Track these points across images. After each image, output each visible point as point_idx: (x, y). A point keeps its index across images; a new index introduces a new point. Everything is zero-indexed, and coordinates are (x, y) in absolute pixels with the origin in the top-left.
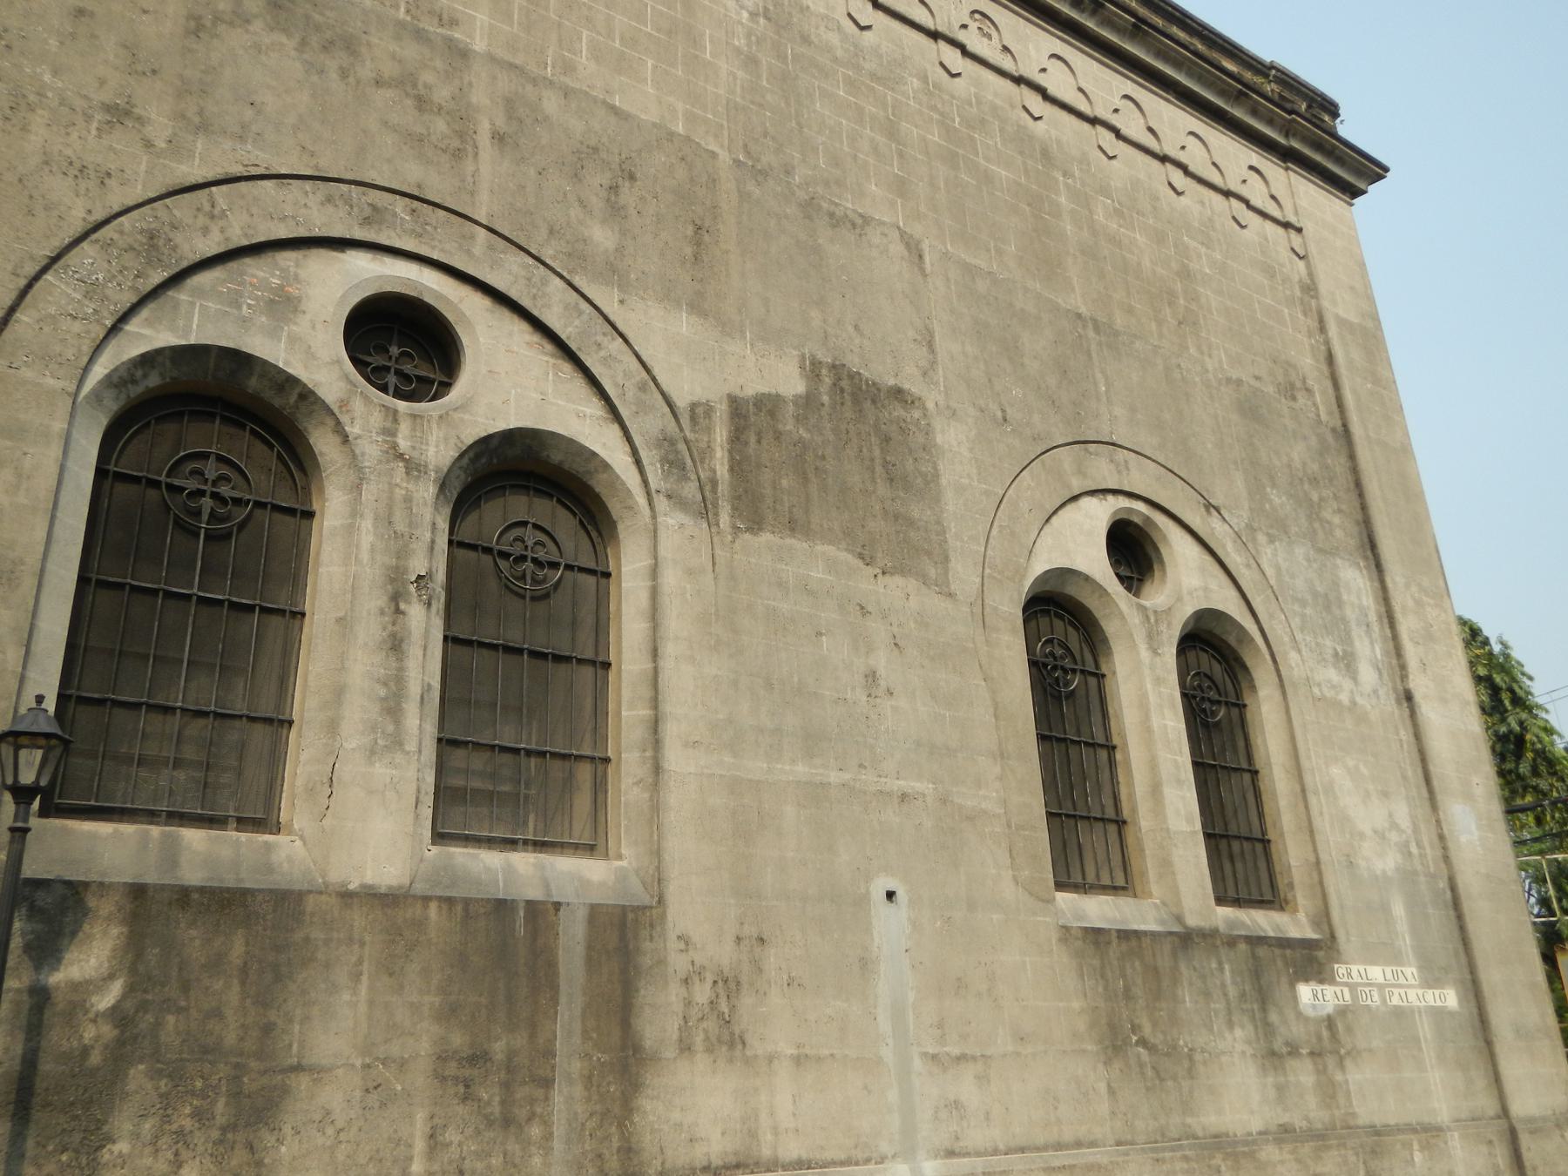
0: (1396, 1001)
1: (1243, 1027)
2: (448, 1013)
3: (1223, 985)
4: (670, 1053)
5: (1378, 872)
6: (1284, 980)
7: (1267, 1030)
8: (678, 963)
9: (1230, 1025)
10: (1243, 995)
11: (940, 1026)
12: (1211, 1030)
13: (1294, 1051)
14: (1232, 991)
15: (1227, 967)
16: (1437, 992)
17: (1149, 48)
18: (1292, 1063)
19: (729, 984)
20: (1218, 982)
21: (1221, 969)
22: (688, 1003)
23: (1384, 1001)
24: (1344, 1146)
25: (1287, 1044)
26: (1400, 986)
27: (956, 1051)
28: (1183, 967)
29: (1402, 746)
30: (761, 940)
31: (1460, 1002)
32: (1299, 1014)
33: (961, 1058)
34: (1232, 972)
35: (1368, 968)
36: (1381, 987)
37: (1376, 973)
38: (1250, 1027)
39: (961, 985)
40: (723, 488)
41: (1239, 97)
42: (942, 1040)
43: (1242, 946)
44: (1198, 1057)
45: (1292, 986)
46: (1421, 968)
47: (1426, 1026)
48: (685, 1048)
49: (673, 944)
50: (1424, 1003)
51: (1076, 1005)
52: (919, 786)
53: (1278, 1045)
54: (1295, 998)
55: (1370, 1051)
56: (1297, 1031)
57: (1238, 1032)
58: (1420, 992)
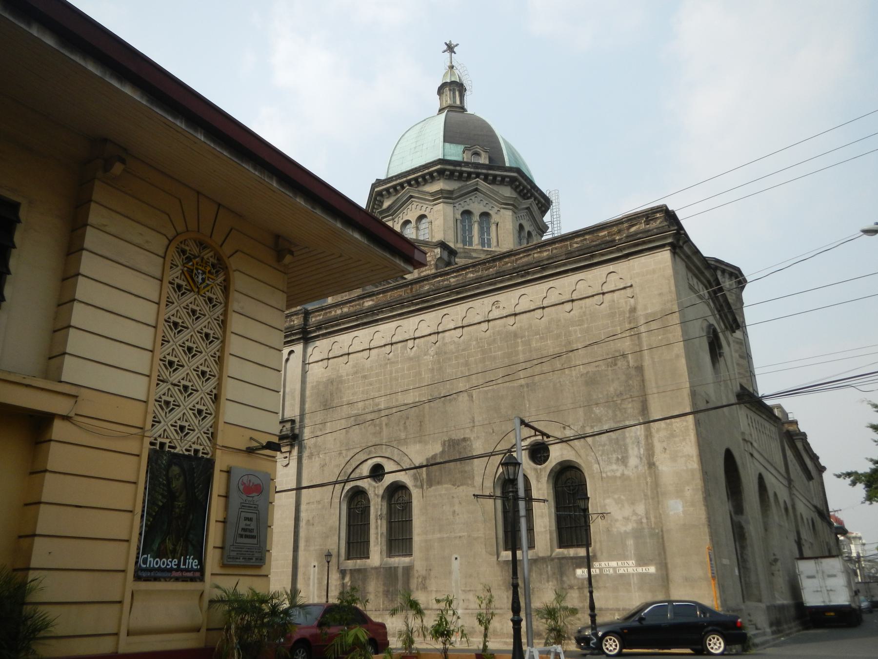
0: (620, 572)
1: (552, 582)
2: (384, 585)
3: (547, 571)
4: (415, 590)
5: (622, 531)
6: (571, 569)
7: (562, 582)
8: (416, 575)
9: (548, 581)
10: (554, 574)
11: (466, 584)
12: (540, 582)
13: (571, 587)
14: (550, 573)
15: (549, 567)
16: (644, 568)
17: (552, 268)
18: (571, 591)
19: (424, 578)
20: (545, 571)
21: (547, 566)
22: (418, 582)
23: (615, 572)
24: (584, 613)
25: (569, 586)
26: (625, 567)
27: (468, 589)
28: (534, 568)
29: (647, 484)
30: (430, 570)
31: (657, 570)
32: (575, 577)
33: (470, 591)
34: (551, 567)
35: (610, 563)
36: (614, 568)
37: (614, 564)
38: (555, 582)
39: (471, 576)
40: (425, 480)
41: (592, 257)
42: (466, 587)
43: (556, 560)
44: (535, 590)
45: (574, 570)
46: (637, 561)
47: (635, 579)
48: (417, 589)
49: (415, 572)
50: (636, 572)
51: (500, 578)
52: (463, 534)
53: (565, 586)
54: (575, 574)
55: (605, 587)
56: (573, 582)
57: (550, 583)
58: (635, 569)
